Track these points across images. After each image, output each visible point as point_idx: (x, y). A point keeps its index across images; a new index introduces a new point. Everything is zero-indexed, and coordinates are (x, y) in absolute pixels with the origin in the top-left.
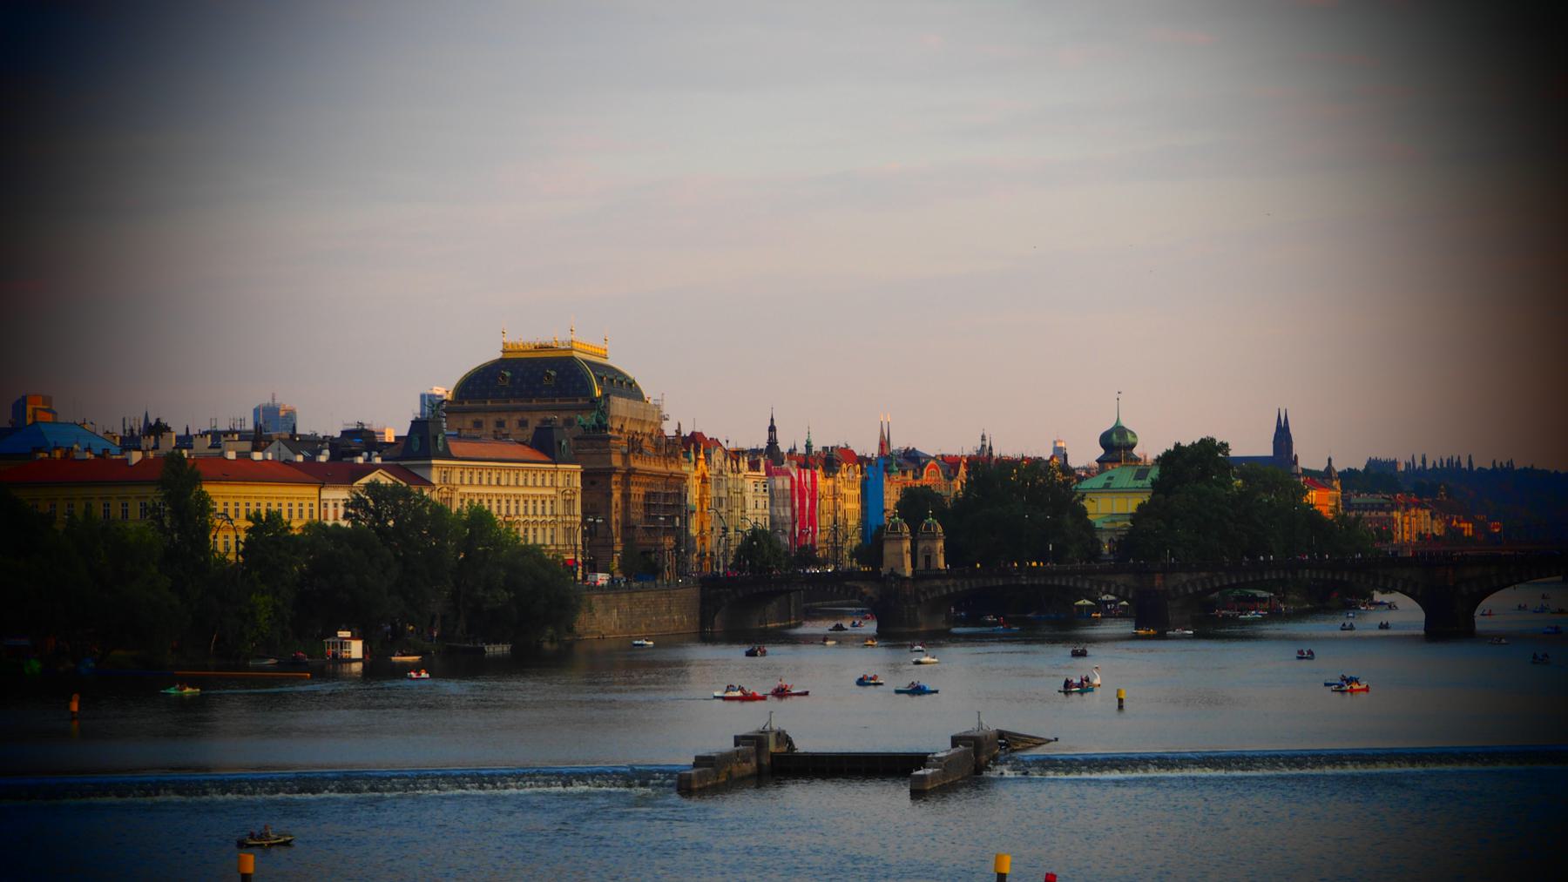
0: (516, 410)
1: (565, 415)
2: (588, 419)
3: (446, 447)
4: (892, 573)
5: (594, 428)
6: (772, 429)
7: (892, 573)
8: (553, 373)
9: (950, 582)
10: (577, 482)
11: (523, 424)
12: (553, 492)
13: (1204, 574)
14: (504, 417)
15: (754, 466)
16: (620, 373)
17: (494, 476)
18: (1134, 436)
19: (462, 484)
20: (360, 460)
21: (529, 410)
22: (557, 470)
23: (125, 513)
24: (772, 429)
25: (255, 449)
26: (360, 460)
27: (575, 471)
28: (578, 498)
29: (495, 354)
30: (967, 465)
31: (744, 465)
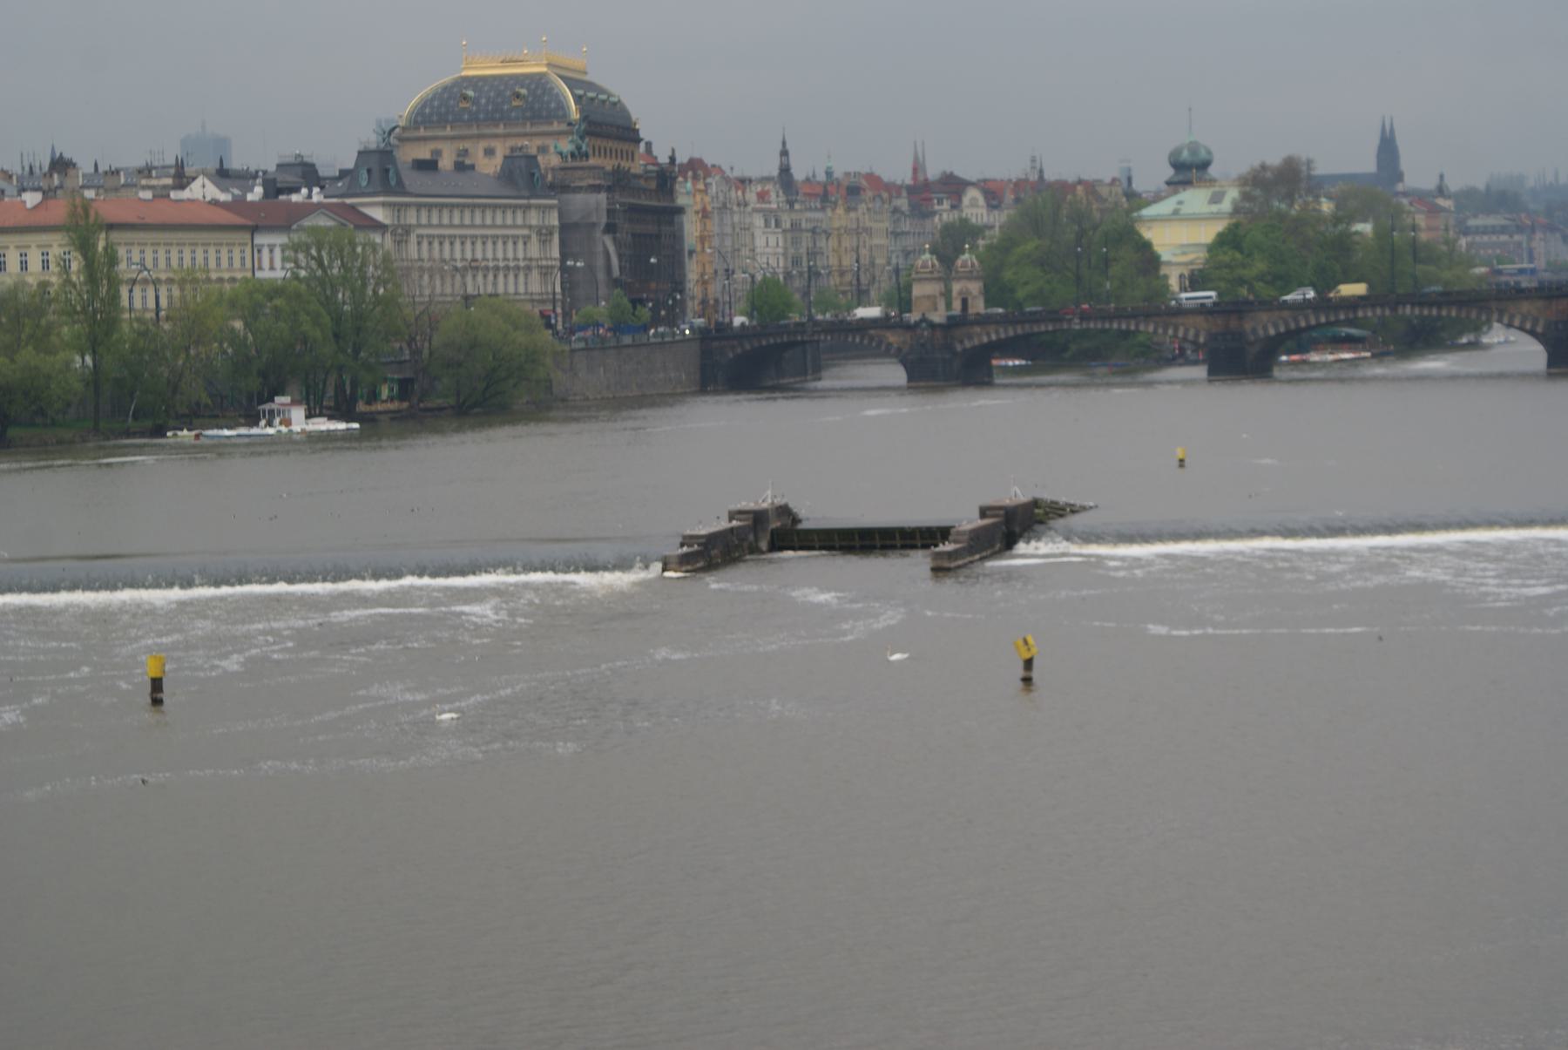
0: (481, 137)
1: (538, 142)
3: (400, 182)
4: (924, 319)
5: (573, 155)
6: (784, 153)
7: (924, 319)
9: (992, 329)
11: (489, 152)
12: (526, 232)
14: (467, 145)
16: (601, 90)
18: (1209, 153)
19: (419, 226)
21: (496, 136)
22: (529, 207)
24: (784, 153)
27: (551, 207)
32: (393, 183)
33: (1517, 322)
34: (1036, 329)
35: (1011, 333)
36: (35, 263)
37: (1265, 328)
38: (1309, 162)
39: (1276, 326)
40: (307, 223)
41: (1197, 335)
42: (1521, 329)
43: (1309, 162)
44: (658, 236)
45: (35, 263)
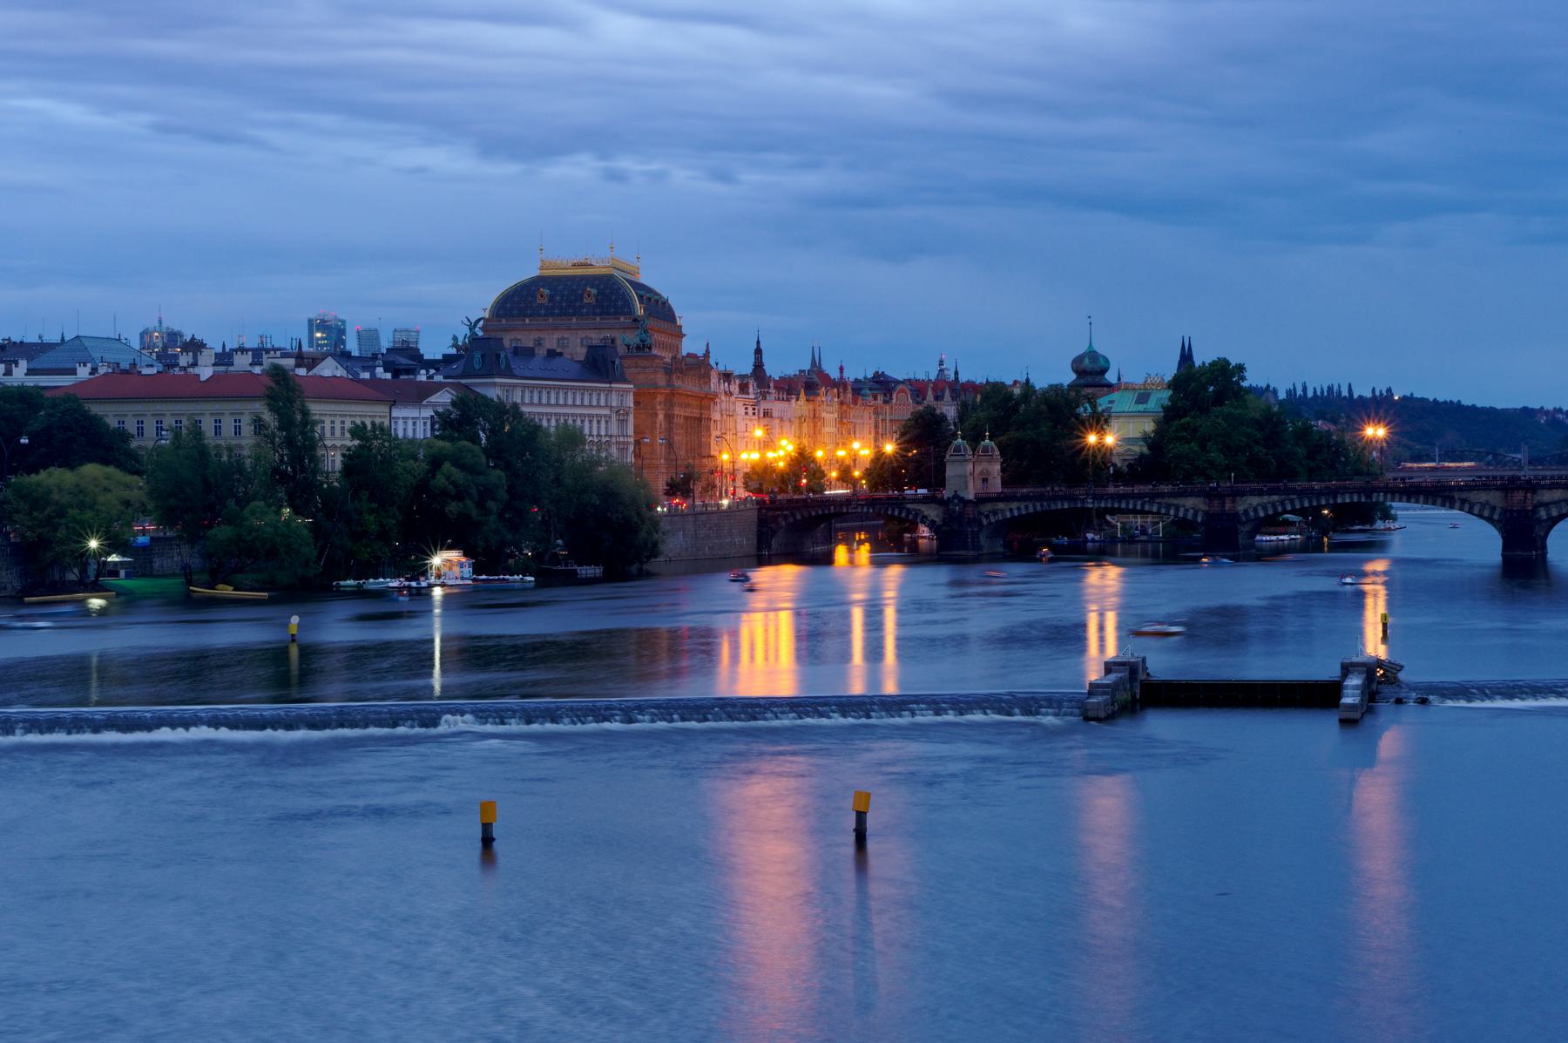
0: (556, 328)
1: (535, 335)
2: (632, 338)
3: (508, 365)
4: (956, 496)
5: (638, 348)
6: (758, 351)
7: (956, 496)
8: (594, 291)
9: (1014, 505)
10: (630, 401)
12: (607, 412)
13: (1275, 498)
14: (543, 335)
15: (743, 388)
16: (656, 293)
17: (527, 394)
18: (1107, 361)
20: (422, 376)
22: (611, 390)
23: (218, 430)
24: (758, 351)
25: (298, 365)
26: (422, 376)
27: (628, 391)
28: (631, 417)
29: (531, 272)
30: (934, 390)
31: (735, 388)
32: (503, 367)
33: (1476, 511)
34: (1053, 507)
35: (1031, 510)
36: (228, 426)
37: (1255, 510)
38: (1240, 368)
39: (1265, 509)
40: (433, 399)
41: (1195, 515)
42: (1480, 516)
43: (1240, 368)
44: (700, 419)
45: (228, 426)
